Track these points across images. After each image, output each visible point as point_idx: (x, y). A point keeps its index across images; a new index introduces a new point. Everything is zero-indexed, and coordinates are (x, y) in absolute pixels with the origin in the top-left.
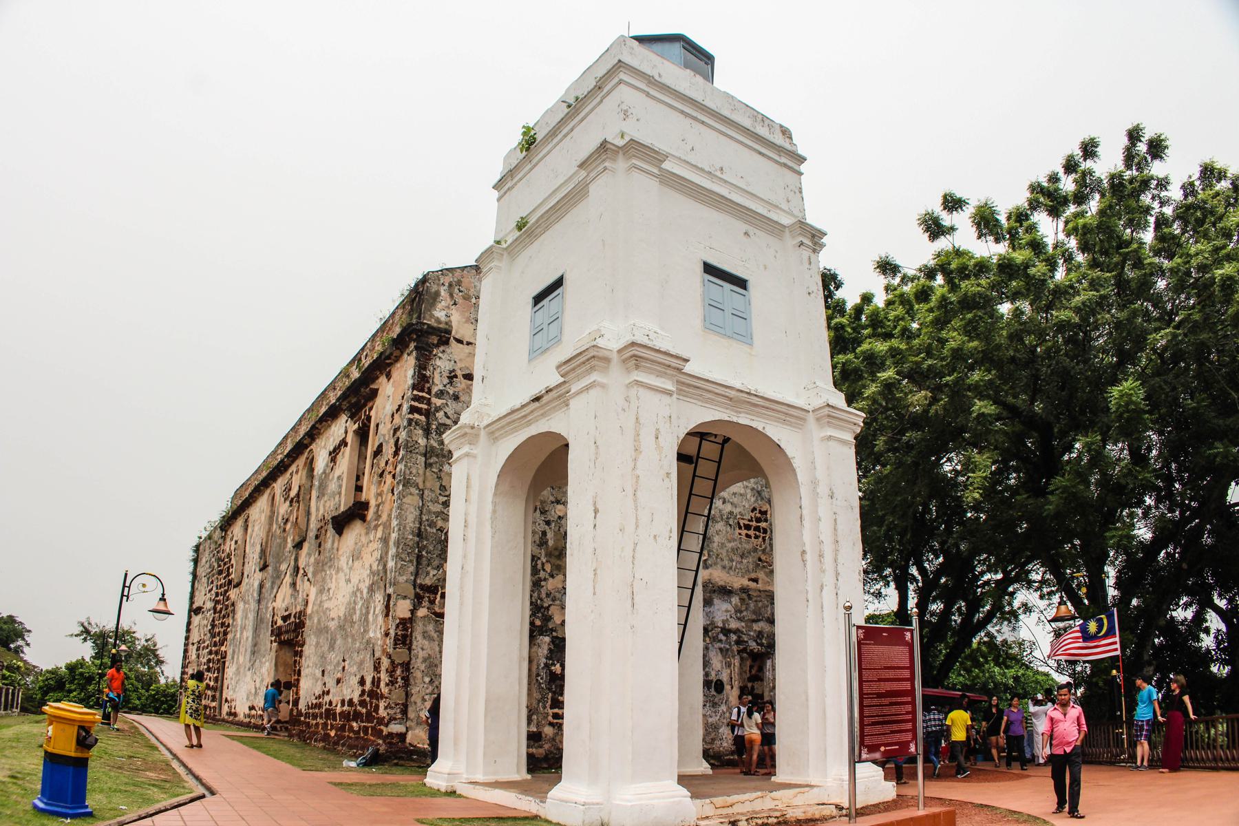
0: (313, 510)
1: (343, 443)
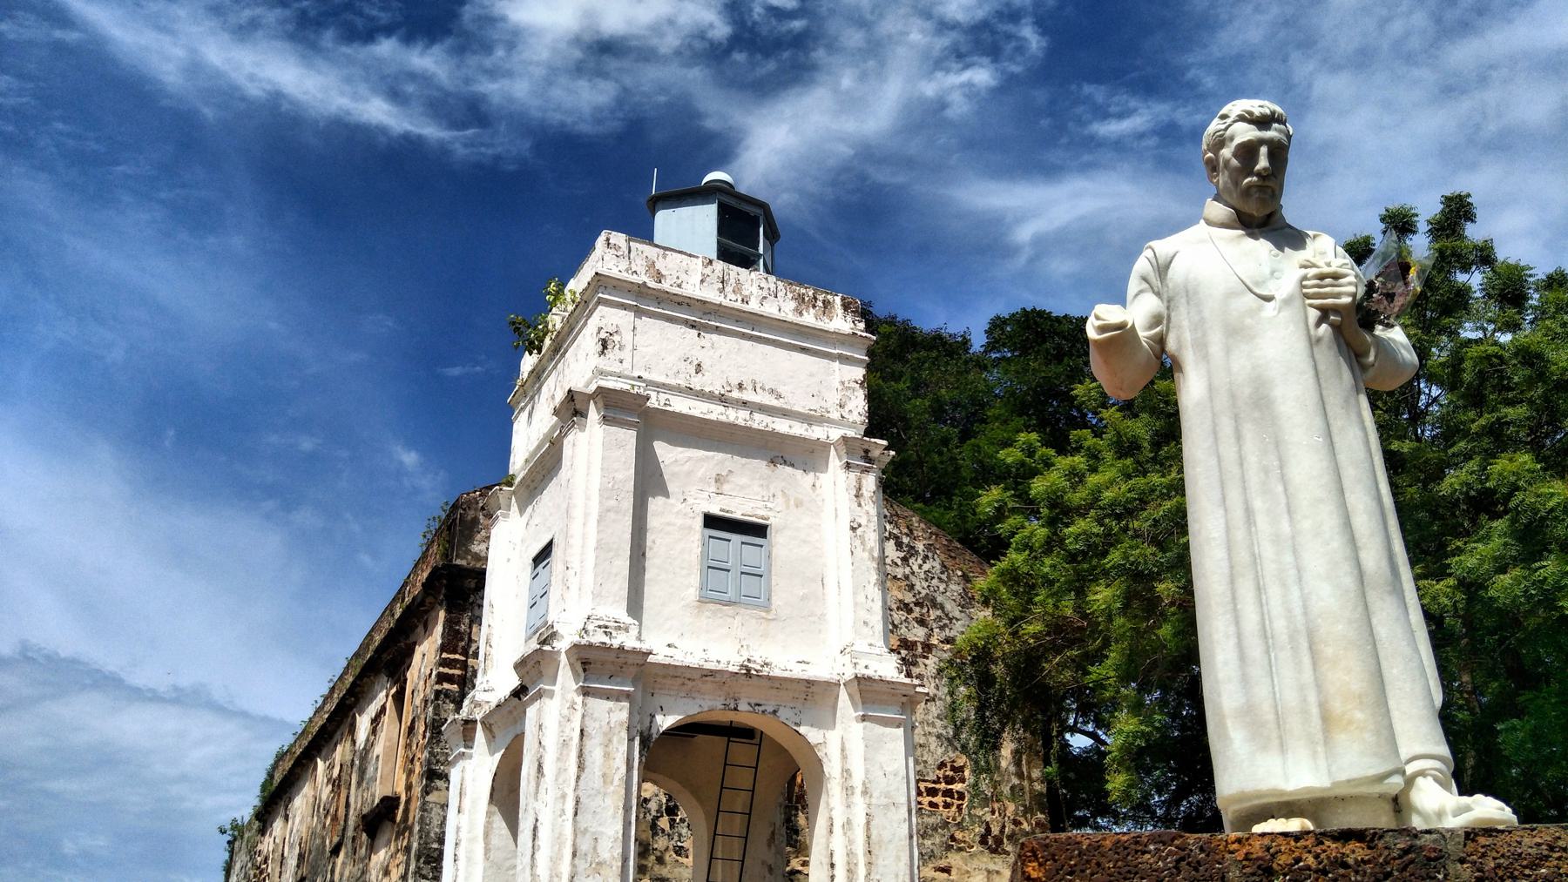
0: (352, 800)
1: (383, 710)
